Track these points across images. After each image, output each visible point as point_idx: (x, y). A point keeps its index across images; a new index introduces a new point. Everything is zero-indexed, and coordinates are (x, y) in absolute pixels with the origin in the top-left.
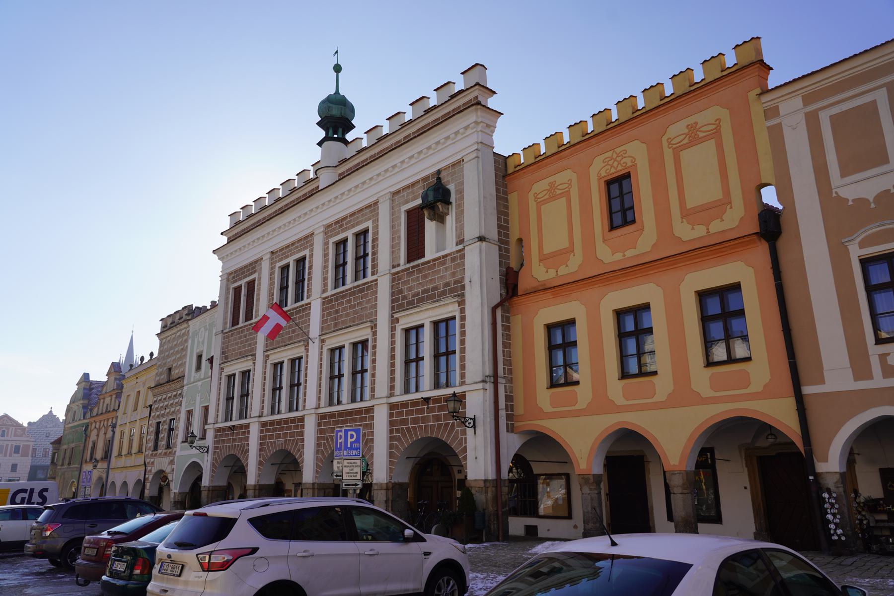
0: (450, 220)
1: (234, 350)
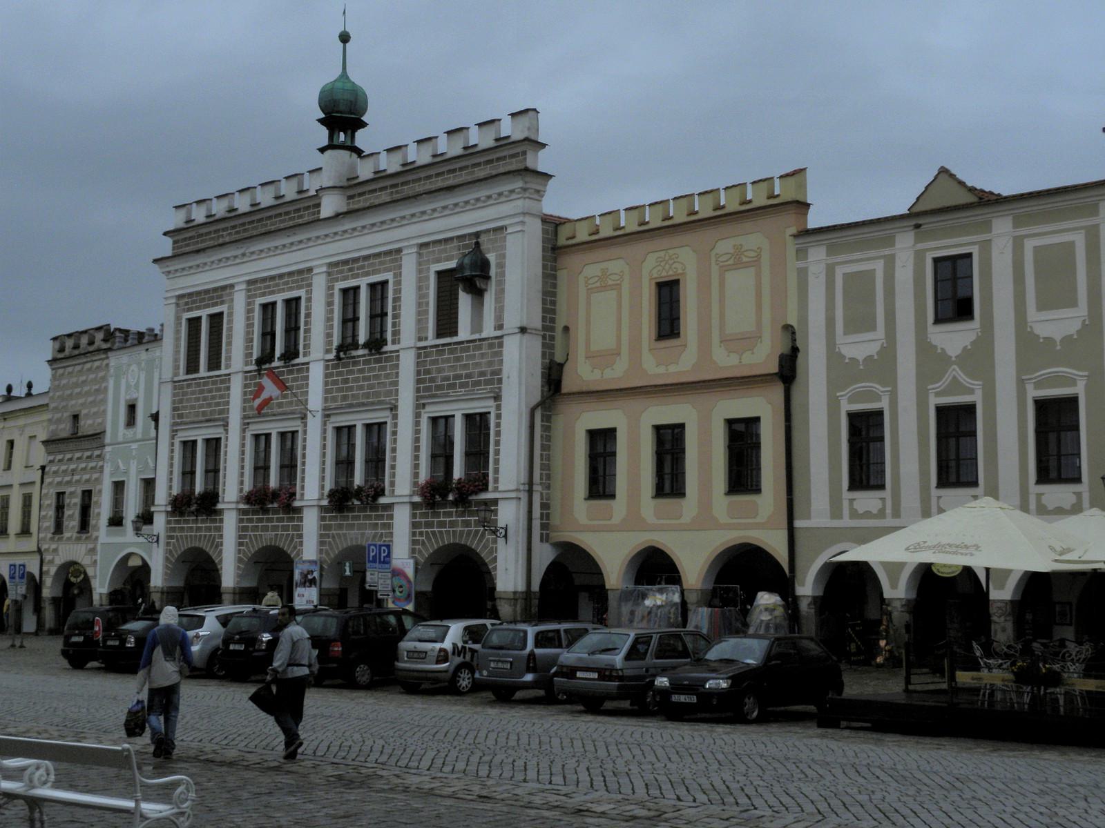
0: (489, 299)
1: (193, 407)
